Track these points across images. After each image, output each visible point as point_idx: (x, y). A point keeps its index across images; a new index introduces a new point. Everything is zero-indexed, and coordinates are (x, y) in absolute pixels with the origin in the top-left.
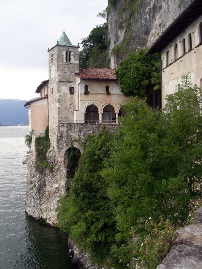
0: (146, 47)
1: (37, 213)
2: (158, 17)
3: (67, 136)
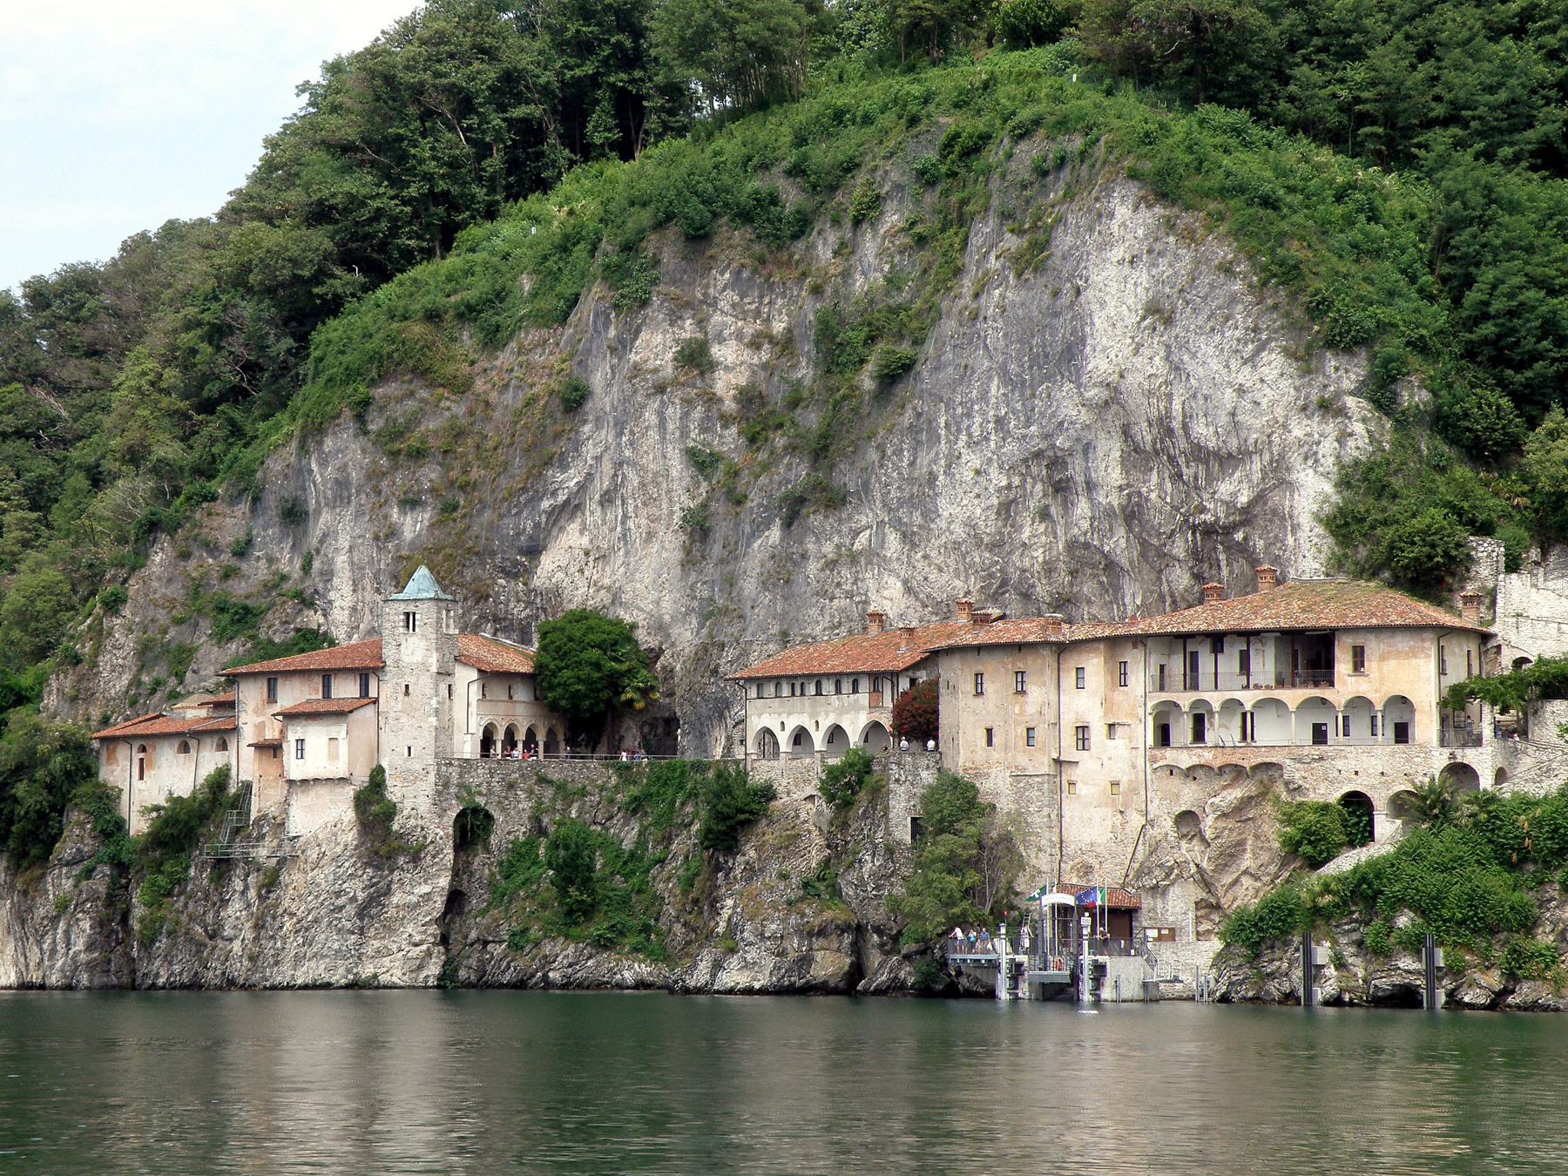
0: (525, 584)
1: (341, 971)
2: (573, 527)
3: (460, 786)
